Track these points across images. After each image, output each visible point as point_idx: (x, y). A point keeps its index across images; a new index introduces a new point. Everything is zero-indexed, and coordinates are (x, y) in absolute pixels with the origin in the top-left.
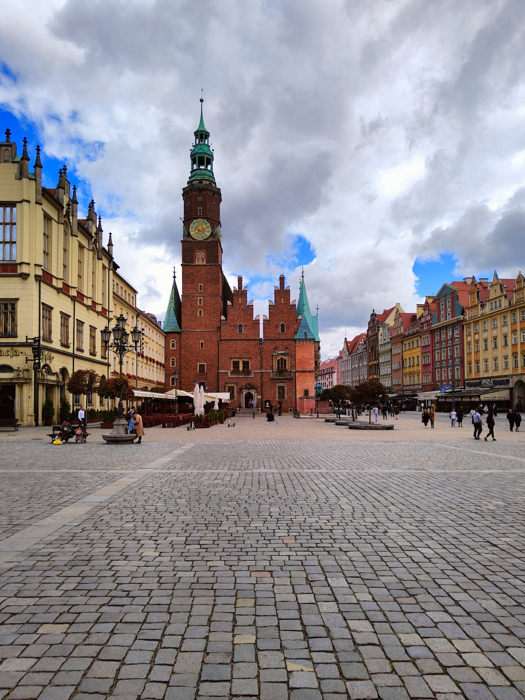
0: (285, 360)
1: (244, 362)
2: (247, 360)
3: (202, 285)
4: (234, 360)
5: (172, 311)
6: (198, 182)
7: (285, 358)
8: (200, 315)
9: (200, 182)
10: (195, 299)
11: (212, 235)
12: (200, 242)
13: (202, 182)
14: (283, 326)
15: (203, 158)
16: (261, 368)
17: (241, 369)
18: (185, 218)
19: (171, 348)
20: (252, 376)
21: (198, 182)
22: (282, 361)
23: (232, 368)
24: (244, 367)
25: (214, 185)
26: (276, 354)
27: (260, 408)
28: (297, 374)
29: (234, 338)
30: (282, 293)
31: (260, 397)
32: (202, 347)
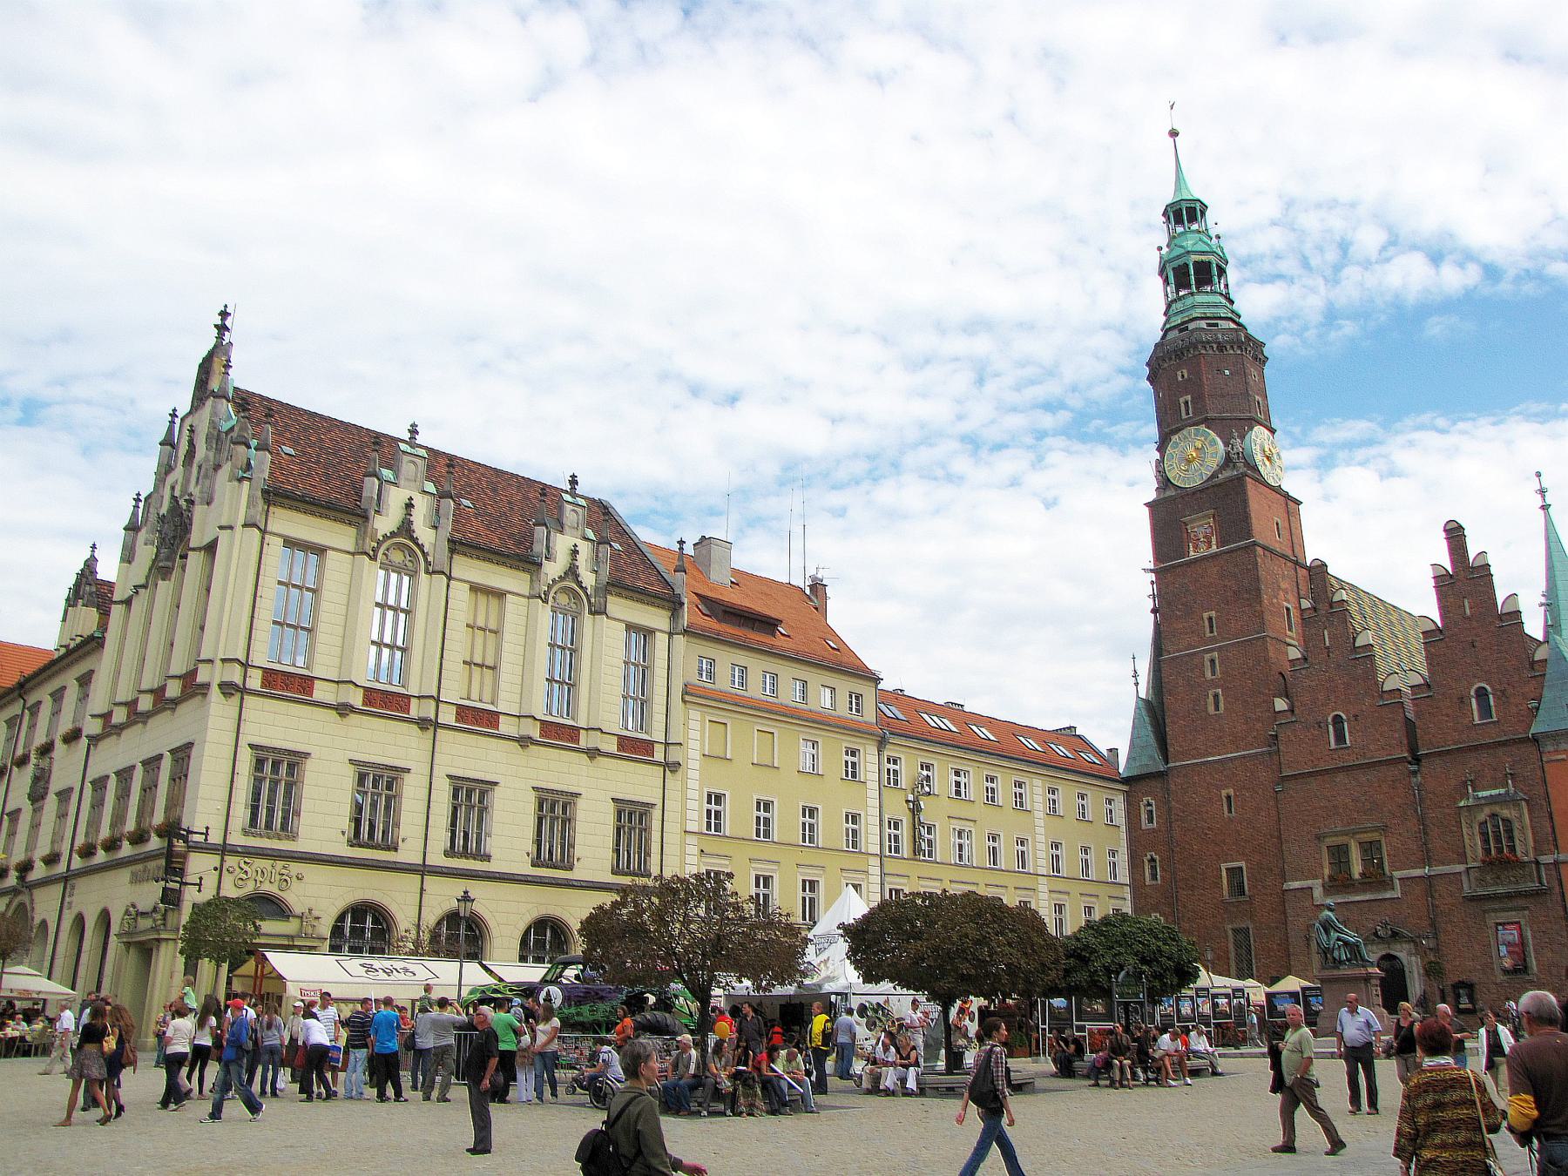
0: (1507, 821)
2: (1375, 836)
3: (1213, 614)
4: (1330, 841)
7: (1505, 813)
8: (1217, 708)
9: (1181, 331)
10: (1196, 661)
11: (1228, 461)
12: (1195, 492)
14: (1481, 694)
15: (1187, 265)
16: (1427, 860)
17: (1357, 869)
19: (1145, 824)
20: (1397, 893)
23: (1327, 872)
26: (1471, 802)
29: (1323, 766)
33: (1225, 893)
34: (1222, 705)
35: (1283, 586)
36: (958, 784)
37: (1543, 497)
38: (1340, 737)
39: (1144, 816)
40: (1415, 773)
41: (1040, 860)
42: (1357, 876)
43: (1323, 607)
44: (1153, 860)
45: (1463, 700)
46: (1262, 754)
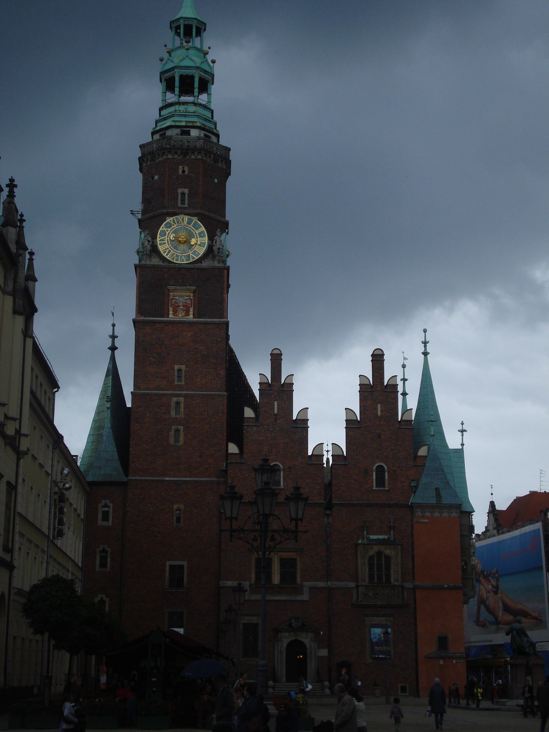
0: (388, 558)
1: (283, 562)
2: (293, 555)
3: (183, 367)
5: (107, 431)
6: (178, 131)
7: (388, 552)
12: (179, 269)
13: (188, 133)
14: (380, 469)
15: (192, 77)
18: (144, 212)
19: (100, 522)
21: (178, 131)
23: (253, 576)
25: (214, 139)
27: (326, 683)
30: (378, 392)
31: (324, 652)
34: (182, 439)
37: (425, 347)
40: (328, 516)
44: (104, 551)
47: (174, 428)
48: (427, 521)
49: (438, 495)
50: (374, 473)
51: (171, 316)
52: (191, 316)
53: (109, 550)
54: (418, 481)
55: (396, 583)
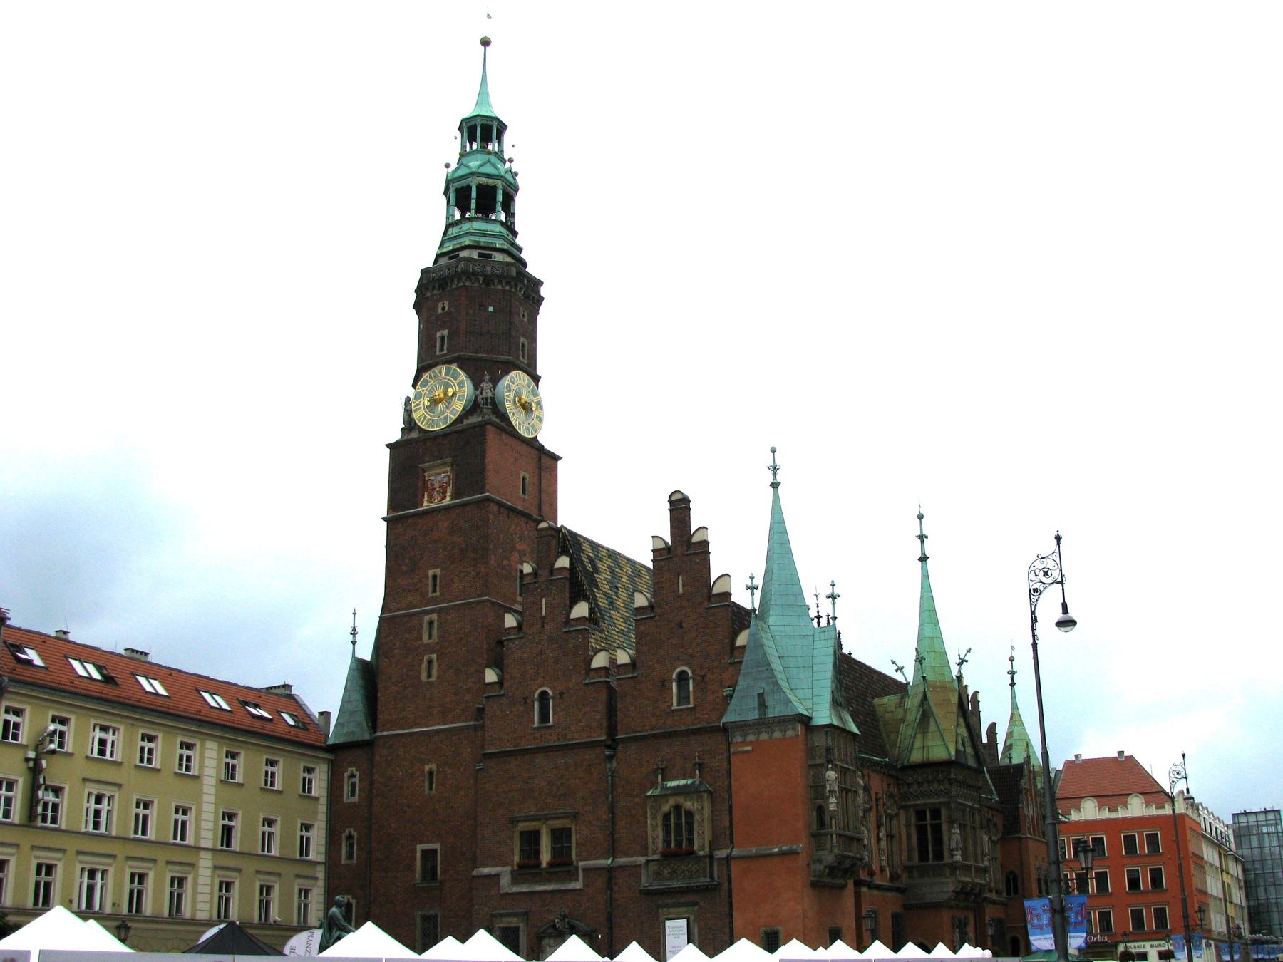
0: (690, 814)
3: (438, 572)
4: (524, 826)
5: (356, 673)
7: (688, 805)
8: (429, 676)
11: (473, 408)
14: (682, 678)
16: (612, 851)
17: (545, 857)
20: (578, 885)
22: (678, 817)
23: (517, 859)
24: (555, 852)
26: (658, 791)
28: (736, 868)
32: (431, 789)
33: (418, 876)
35: (519, 547)
36: (102, 742)
38: (544, 717)
39: (346, 788)
40: (610, 758)
41: (204, 830)
42: (544, 865)
43: (544, 574)
44: (350, 837)
45: (664, 684)
46: (468, 727)
47: (426, 657)
48: (749, 748)
49: (762, 705)
50: (674, 685)
51: (425, 504)
52: (448, 498)
53: (355, 834)
54: (733, 687)
55: (701, 853)
